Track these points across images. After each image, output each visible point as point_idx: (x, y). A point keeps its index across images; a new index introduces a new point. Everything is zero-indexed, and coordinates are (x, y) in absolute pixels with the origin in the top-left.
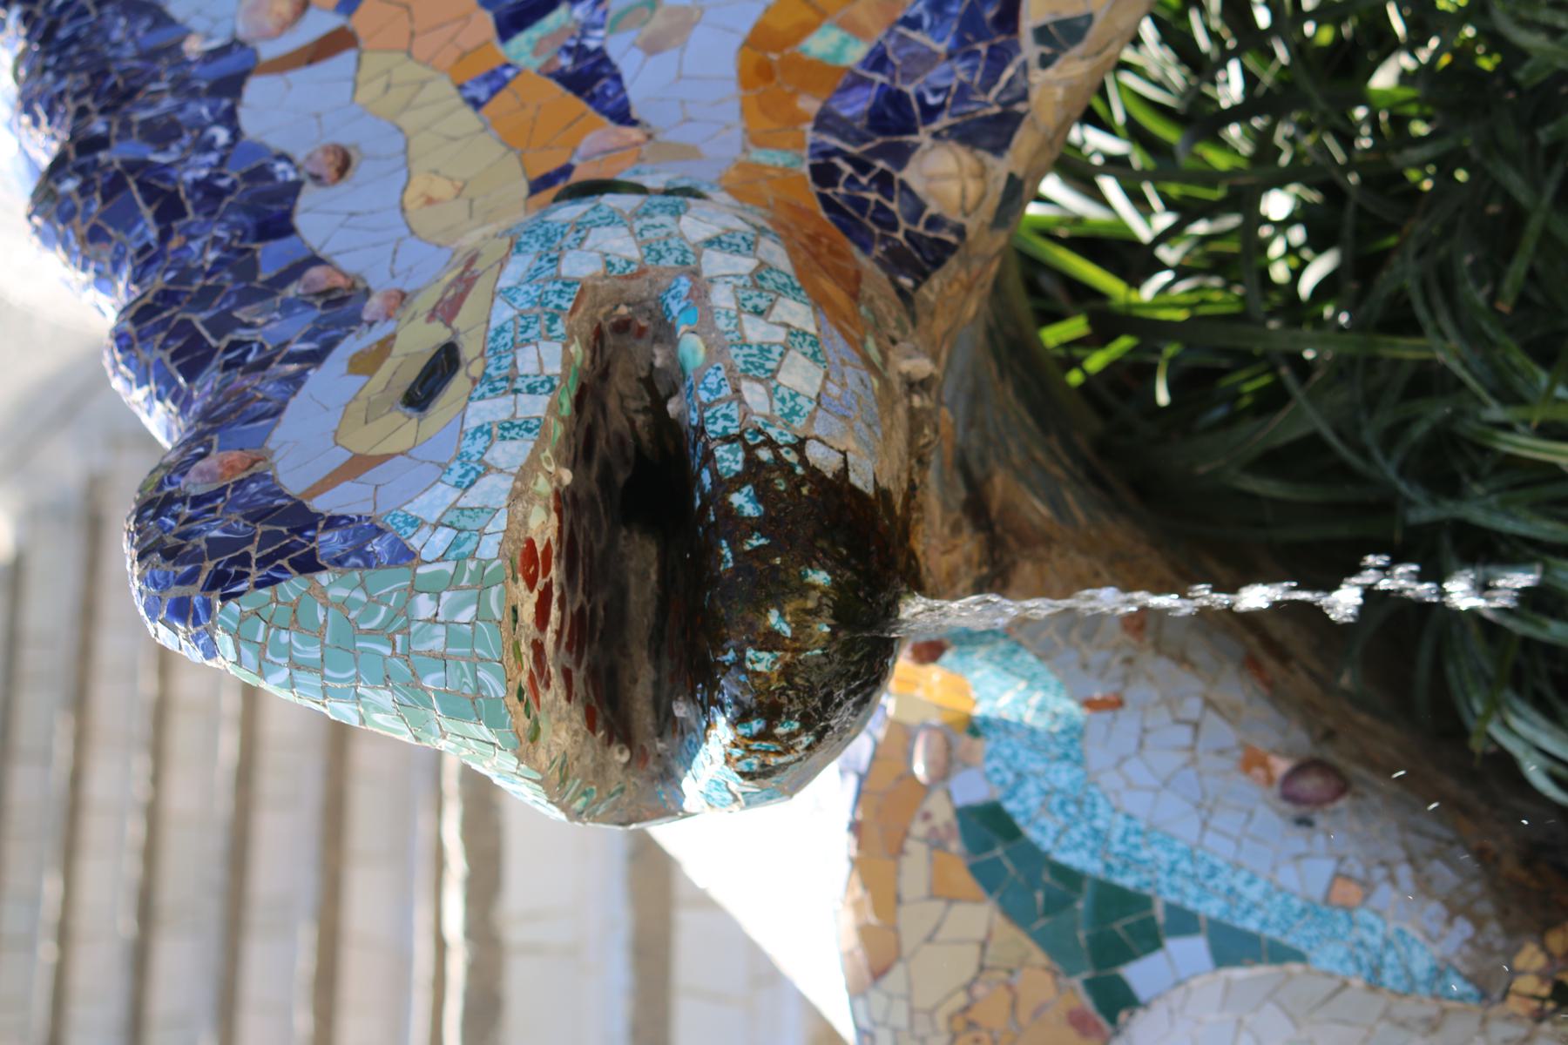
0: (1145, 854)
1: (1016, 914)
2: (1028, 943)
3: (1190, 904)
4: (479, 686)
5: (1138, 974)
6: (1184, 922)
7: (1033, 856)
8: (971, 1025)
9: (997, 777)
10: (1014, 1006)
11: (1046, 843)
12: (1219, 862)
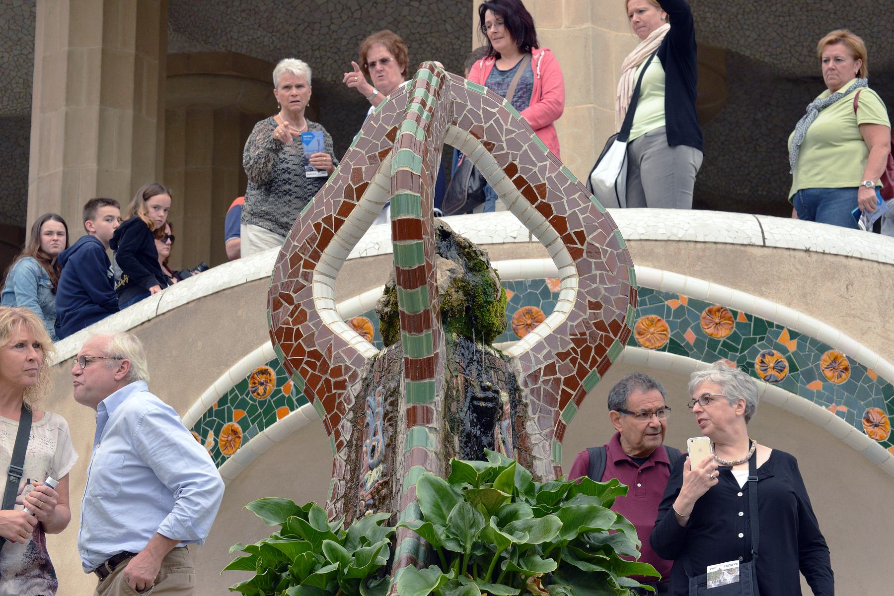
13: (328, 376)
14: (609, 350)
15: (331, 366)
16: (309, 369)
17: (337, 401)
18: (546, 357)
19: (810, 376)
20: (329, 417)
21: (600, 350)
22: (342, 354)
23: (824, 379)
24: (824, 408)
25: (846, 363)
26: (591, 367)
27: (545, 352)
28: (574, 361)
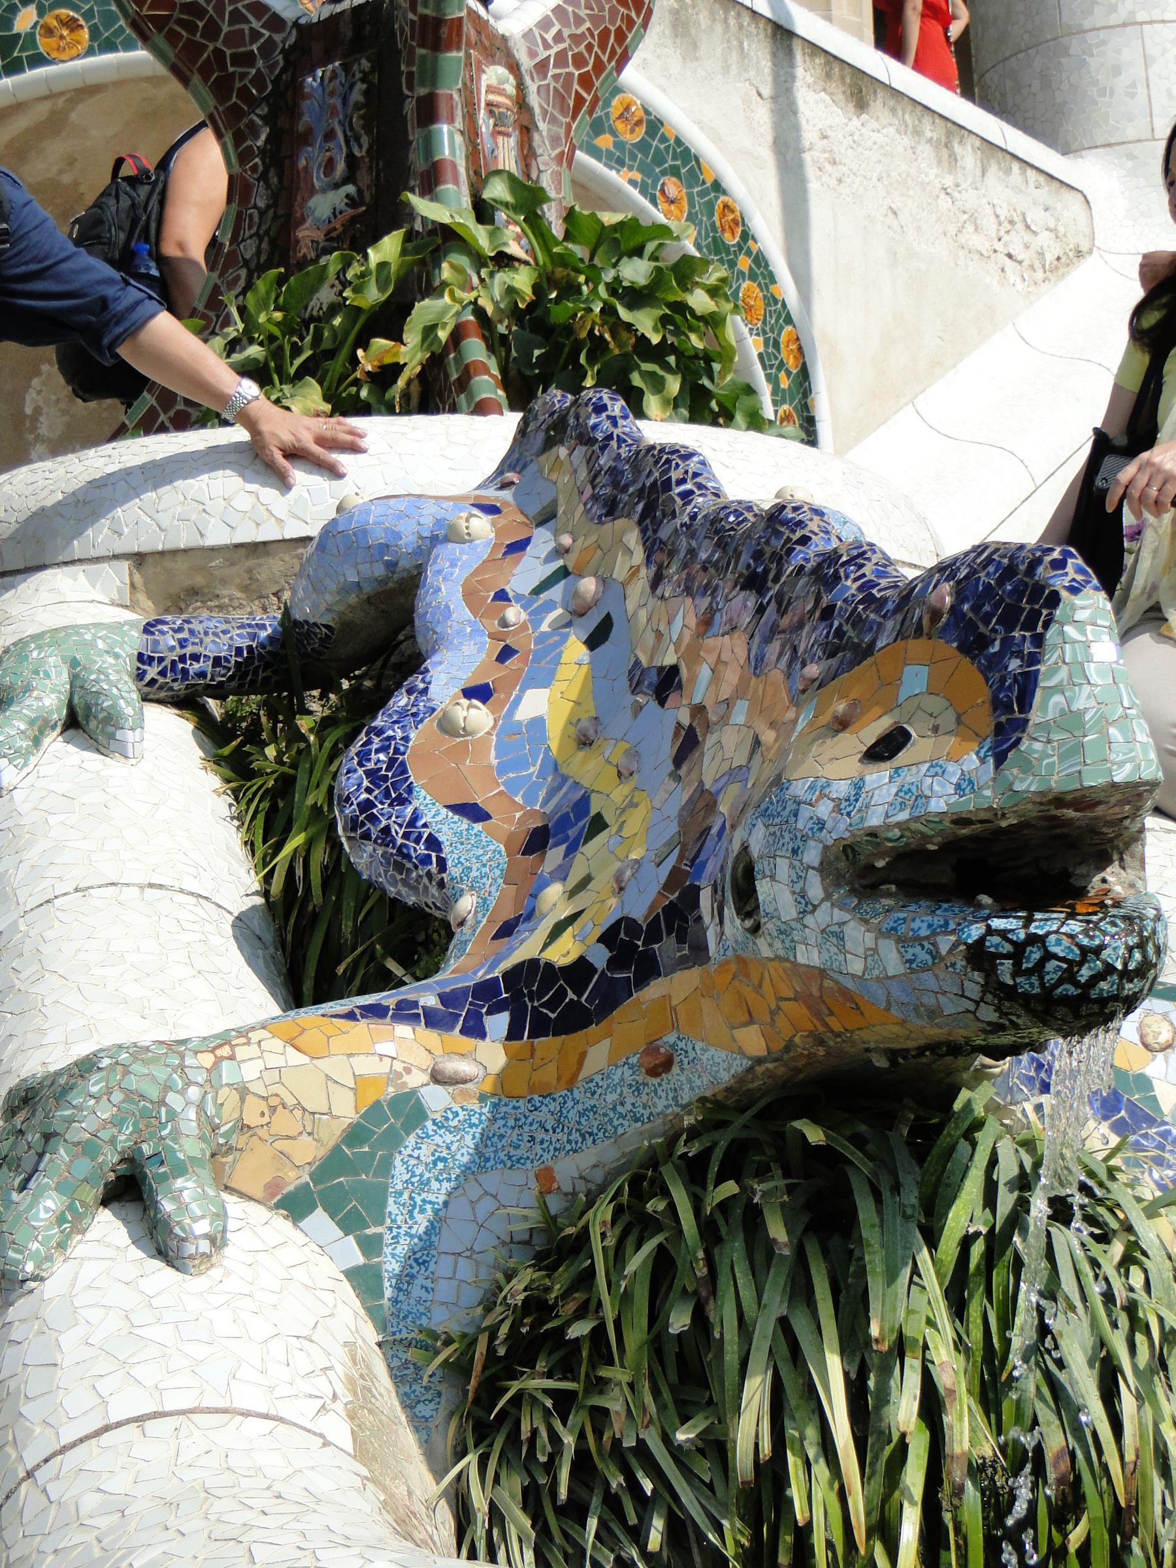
0: (418, 1217)
1: (355, 1134)
2: (331, 1144)
3: (387, 1250)
4: (1121, 764)
5: (319, 1218)
6: (370, 1246)
7: (393, 1141)
8: (273, 1109)
9: (451, 1116)
10: (289, 1137)
11: (406, 1152)
12: (432, 1267)
13: (219, 44)
14: (630, 36)
15: (225, 28)
16: (184, 33)
17: (238, 85)
18: (558, 38)
19: (598, 128)
20: (221, 109)
21: (621, 36)
22: (244, 11)
23: (614, 133)
24: (614, 173)
25: (641, 114)
26: (610, 60)
27: (554, 31)
28: (589, 47)
